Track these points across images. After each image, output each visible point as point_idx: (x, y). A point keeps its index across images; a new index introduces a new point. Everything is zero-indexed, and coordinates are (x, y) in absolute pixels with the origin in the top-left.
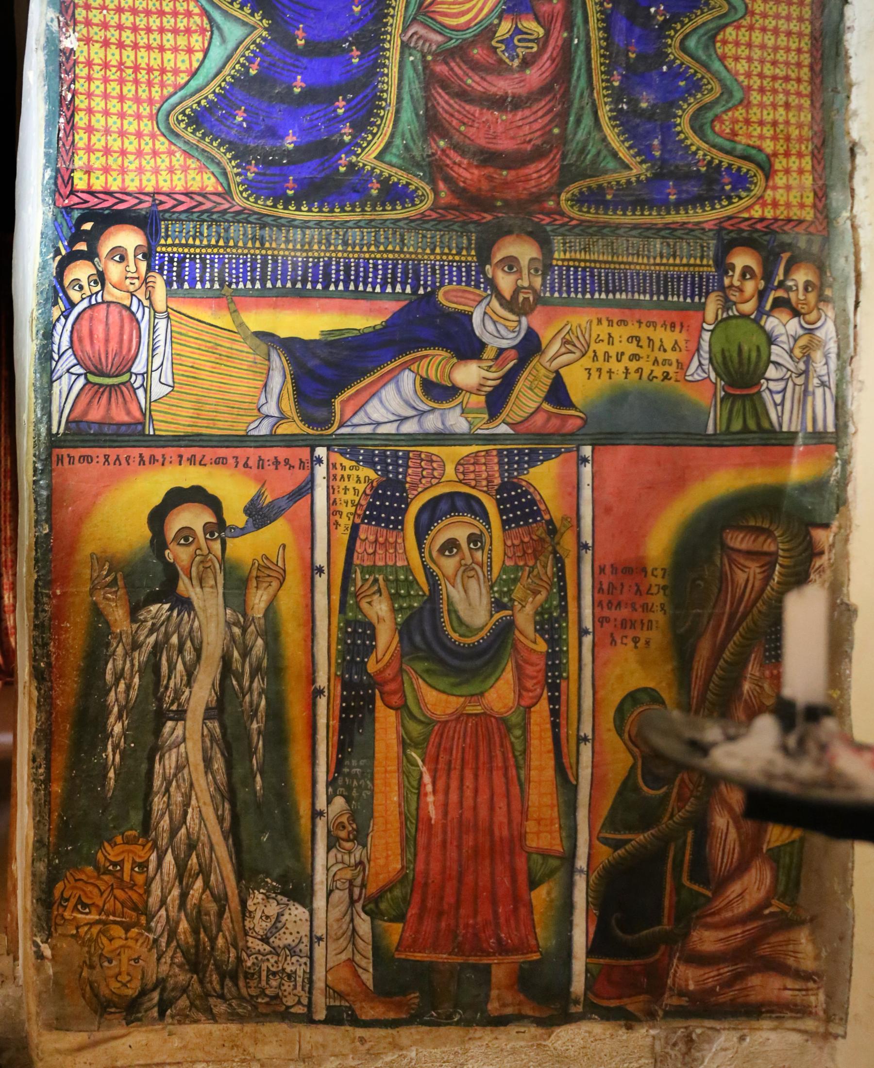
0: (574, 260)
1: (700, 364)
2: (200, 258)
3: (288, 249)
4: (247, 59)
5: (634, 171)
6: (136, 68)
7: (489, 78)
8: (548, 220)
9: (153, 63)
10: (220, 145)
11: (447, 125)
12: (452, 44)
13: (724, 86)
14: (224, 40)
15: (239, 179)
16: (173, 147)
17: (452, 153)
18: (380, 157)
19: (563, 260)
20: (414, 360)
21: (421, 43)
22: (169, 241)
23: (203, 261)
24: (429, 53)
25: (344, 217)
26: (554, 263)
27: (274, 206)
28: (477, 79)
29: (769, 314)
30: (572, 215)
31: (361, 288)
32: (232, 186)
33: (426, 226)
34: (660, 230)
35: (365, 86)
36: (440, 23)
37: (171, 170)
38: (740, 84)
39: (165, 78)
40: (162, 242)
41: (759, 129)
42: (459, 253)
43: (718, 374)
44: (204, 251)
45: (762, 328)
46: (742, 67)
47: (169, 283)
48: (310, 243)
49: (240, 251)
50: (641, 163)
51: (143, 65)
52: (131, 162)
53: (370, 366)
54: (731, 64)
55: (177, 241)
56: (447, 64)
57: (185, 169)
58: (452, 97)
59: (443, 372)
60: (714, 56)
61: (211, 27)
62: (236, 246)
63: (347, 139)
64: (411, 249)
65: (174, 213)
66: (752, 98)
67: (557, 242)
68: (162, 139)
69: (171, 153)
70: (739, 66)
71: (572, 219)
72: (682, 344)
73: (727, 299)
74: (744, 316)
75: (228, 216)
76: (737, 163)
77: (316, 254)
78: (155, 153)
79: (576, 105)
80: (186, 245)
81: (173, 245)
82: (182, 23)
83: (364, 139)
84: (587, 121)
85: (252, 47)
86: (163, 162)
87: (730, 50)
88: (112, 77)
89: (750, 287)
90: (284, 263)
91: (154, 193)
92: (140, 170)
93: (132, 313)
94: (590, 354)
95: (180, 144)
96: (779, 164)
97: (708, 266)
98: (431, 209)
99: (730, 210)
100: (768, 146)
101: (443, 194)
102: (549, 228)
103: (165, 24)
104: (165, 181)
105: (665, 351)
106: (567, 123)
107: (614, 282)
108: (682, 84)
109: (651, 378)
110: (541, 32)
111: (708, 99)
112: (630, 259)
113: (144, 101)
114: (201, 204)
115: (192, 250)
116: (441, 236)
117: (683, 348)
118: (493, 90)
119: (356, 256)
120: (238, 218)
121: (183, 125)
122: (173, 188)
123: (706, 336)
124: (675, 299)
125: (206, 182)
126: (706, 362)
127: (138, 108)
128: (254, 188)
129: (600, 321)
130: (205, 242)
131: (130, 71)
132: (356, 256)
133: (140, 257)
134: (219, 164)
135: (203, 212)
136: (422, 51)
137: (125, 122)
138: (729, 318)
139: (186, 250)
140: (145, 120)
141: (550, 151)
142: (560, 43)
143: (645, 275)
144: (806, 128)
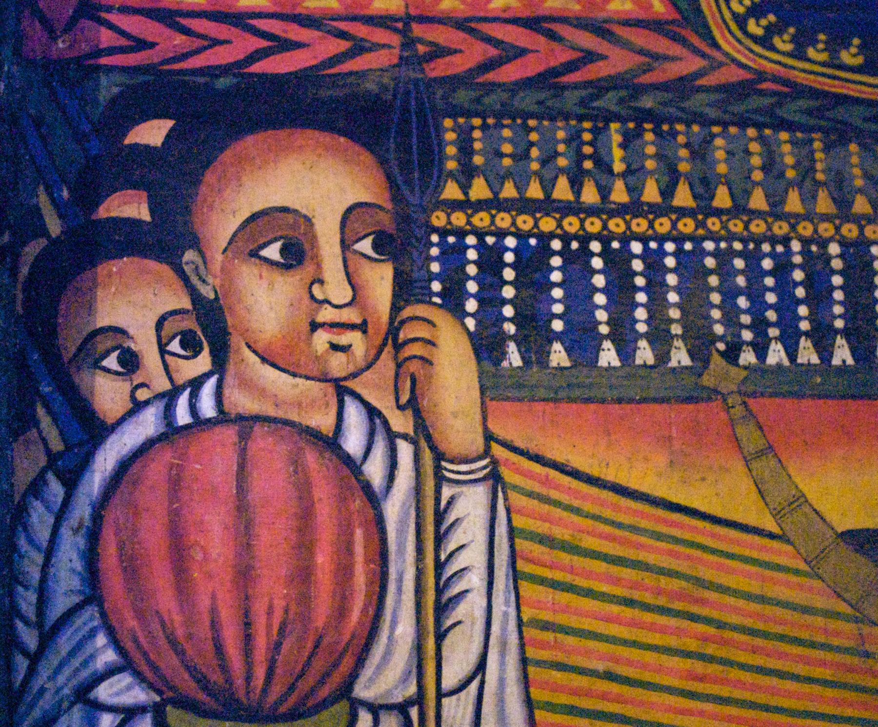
2: (606, 253)
22: (479, 190)
40: (452, 191)
44: (616, 225)
55: (509, 191)
62: (739, 209)
75: (697, 102)
81: (495, 204)
91: (408, 19)
93: (347, 460)
114: (589, 57)
120: (739, 108)
133: (365, 246)
135: (600, 87)
139: (548, 224)
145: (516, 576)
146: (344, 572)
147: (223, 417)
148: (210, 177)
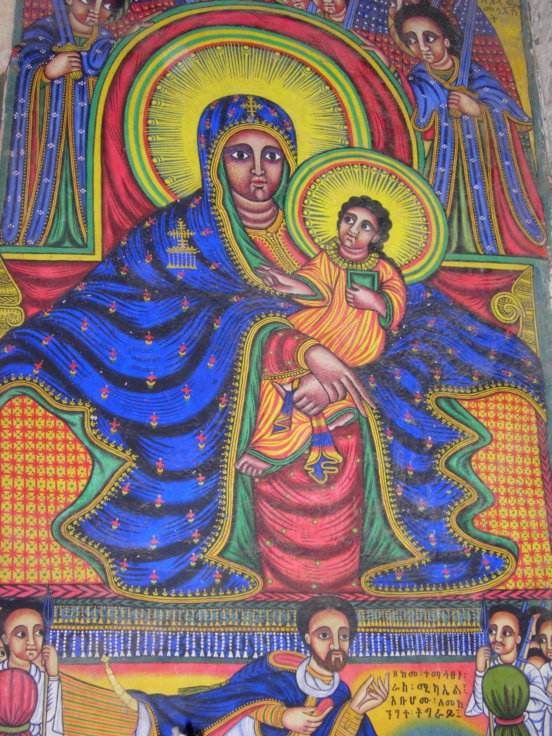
0: (374, 627)
1: (476, 703)
2: (85, 634)
3: (152, 626)
4: (120, 483)
5: (417, 558)
6: (37, 492)
7: (303, 493)
8: (352, 597)
9: (49, 488)
10: (100, 547)
11: (272, 530)
12: (274, 469)
13: (479, 493)
14: (102, 470)
15: (114, 573)
16: (63, 550)
17: (276, 550)
18: (220, 555)
19: (365, 628)
20: (253, 709)
21: (250, 469)
22: (61, 621)
23: (87, 636)
24: (256, 477)
25: (194, 600)
26: (359, 630)
27: (142, 593)
28: (294, 494)
29: (527, 661)
30: (371, 593)
31: (209, 654)
32: (109, 578)
33: (258, 606)
34: (439, 601)
35: (208, 503)
36: (264, 455)
37: (62, 567)
38: (491, 491)
39: (58, 498)
40: (55, 621)
41: (507, 524)
42: (284, 626)
43: (490, 710)
44: (87, 628)
45: (522, 673)
46: (492, 479)
47: (60, 653)
48: (169, 621)
49: (115, 628)
50: (421, 552)
51: (42, 490)
52: (32, 561)
53: (218, 715)
54: (483, 476)
55: (66, 621)
56: (270, 484)
57: (73, 566)
58: (275, 508)
59: (276, 717)
60: (471, 472)
61: (93, 461)
62: (112, 624)
63: (196, 541)
64: (247, 624)
65: (64, 599)
66: (500, 501)
67: (360, 614)
68: (55, 543)
69: (62, 554)
70: (489, 478)
71: (371, 596)
72: (461, 688)
73: (493, 653)
74: (507, 664)
76: (493, 549)
77: (174, 629)
78: (50, 554)
79: (369, 511)
80: (74, 624)
81: (63, 624)
82: (71, 459)
83: (209, 541)
84: (378, 522)
85: (124, 475)
86: (56, 561)
87: (482, 467)
88: (18, 499)
89: (510, 642)
90: (150, 637)
91: (49, 585)
92: (39, 567)
93: (31, 677)
94: (390, 699)
95: (69, 547)
96: (525, 548)
97: (477, 627)
98: (261, 593)
99: (491, 585)
100: (515, 535)
101: (270, 581)
102: (353, 604)
103: (58, 459)
104: (57, 575)
105: (448, 694)
106: (363, 525)
107: (405, 644)
108: (449, 492)
109: (438, 715)
110: (341, 459)
111: (468, 503)
112: (417, 625)
113: (42, 515)
114: (84, 592)
115: (78, 628)
116: (270, 613)
117: (462, 691)
118: (307, 501)
119: (205, 630)
120: (114, 602)
121: (71, 533)
122: (63, 581)
123: (479, 681)
124: (454, 653)
125: (89, 575)
126: (480, 701)
127: (38, 521)
128: (125, 579)
129: (395, 674)
130: (88, 621)
131: (32, 494)
132: (205, 630)
133: (37, 633)
134: (99, 562)
135: (86, 599)
136: (251, 476)
137: (28, 532)
138: (495, 666)
139: (73, 628)
140: (43, 530)
141: (352, 546)
142: (354, 467)
143: (429, 637)
144: (543, 521)
145: (62, 699)
146: (30, 699)
147: (9, 668)
148: (8, 619)
